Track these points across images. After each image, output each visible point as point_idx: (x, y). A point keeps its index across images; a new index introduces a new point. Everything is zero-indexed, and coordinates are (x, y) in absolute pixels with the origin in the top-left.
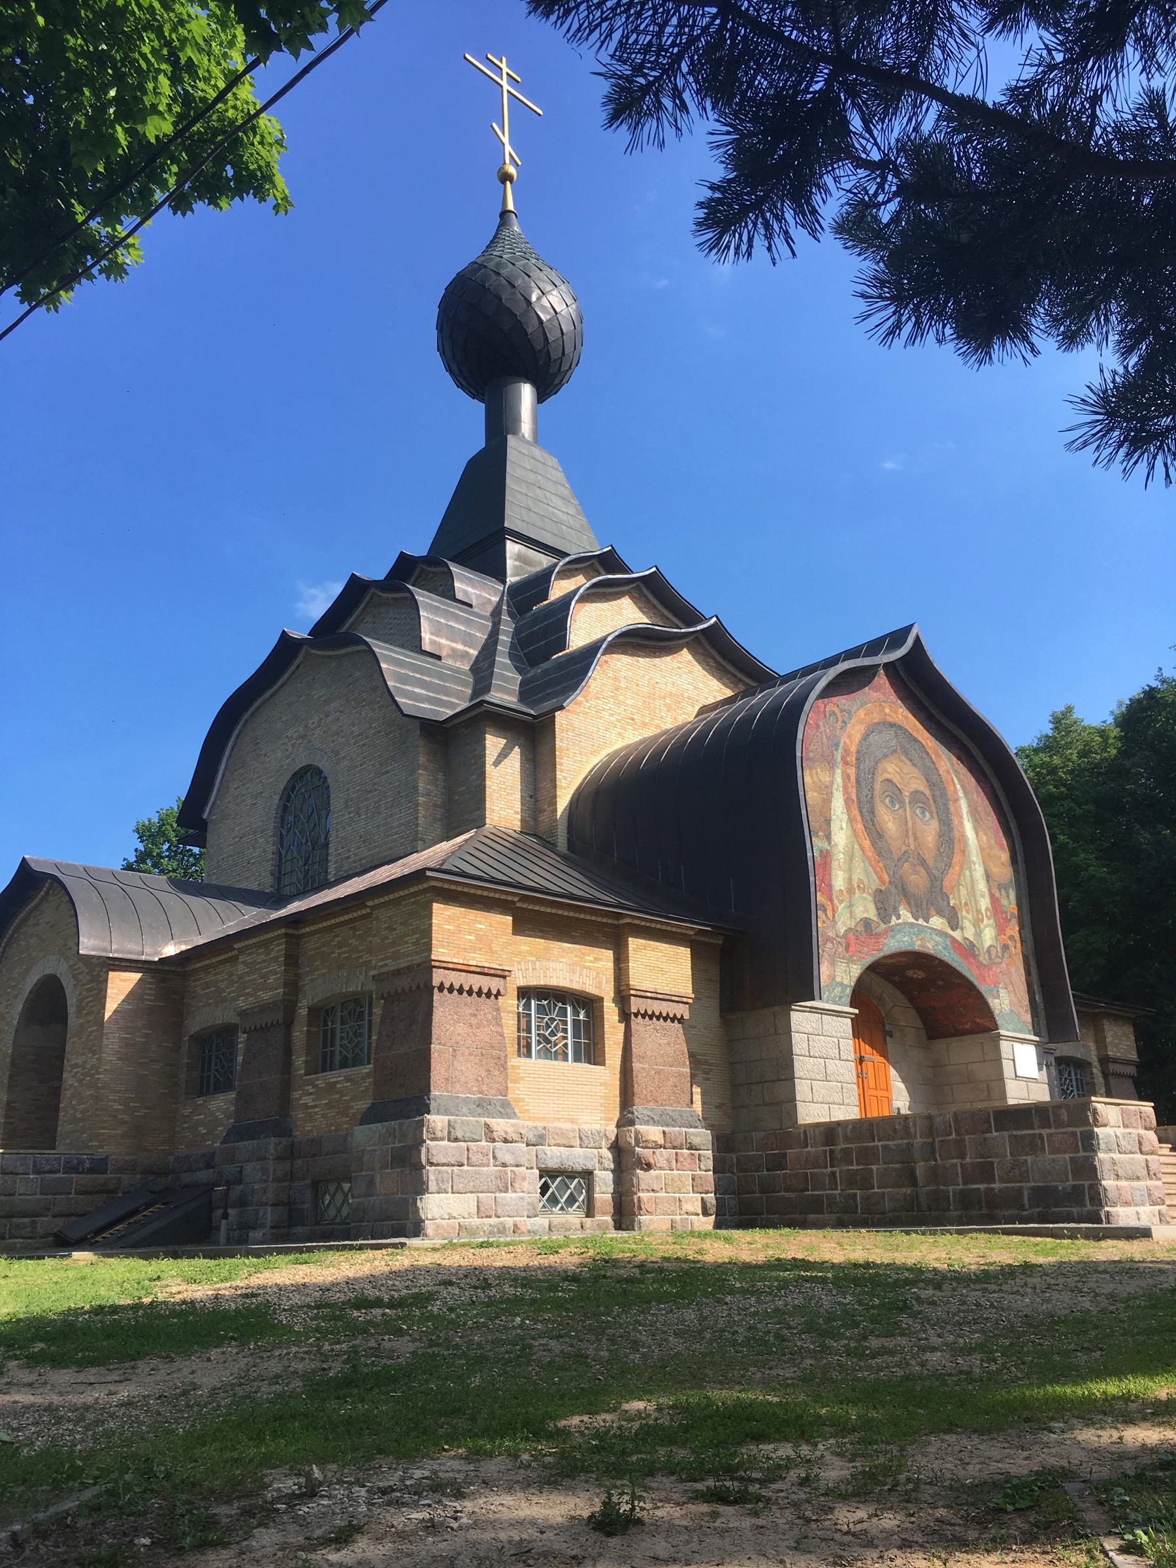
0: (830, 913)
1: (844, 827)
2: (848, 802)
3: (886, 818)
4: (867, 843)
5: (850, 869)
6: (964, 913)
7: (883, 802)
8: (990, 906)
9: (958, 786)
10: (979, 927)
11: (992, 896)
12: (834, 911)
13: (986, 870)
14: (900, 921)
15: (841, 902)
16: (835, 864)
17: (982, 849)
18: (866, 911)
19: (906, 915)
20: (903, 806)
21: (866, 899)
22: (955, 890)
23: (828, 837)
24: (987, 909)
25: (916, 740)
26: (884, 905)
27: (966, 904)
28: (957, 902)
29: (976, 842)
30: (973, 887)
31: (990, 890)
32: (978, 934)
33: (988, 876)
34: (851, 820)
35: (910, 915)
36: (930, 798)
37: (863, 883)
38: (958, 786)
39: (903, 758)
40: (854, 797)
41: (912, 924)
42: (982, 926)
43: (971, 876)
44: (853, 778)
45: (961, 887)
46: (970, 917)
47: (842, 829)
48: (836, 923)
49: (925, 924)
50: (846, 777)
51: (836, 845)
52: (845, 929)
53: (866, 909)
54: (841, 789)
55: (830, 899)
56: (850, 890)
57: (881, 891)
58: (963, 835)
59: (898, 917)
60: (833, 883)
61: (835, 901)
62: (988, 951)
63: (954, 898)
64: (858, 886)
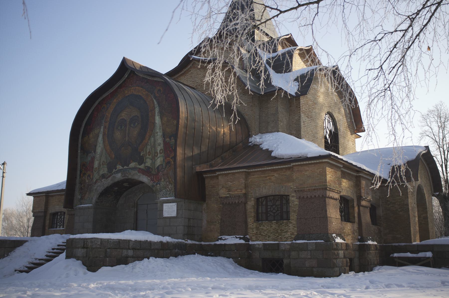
0: (91, 176)
1: (101, 145)
5: (100, 159)
6: (148, 156)
8: (163, 148)
9: (156, 103)
11: (165, 143)
13: (163, 132)
14: (117, 170)
16: (96, 159)
17: (163, 124)
19: (119, 167)
23: (95, 152)
26: (111, 167)
27: (149, 152)
28: (145, 152)
29: (160, 123)
32: (153, 163)
33: (164, 136)
34: (104, 142)
35: (121, 166)
37: (104, 162)
38: (156, 103)
40: (106, 133)
41: (122, 169)
42: (156, 158)
44: (107, 127)
46: (151, 156)
47: (100, 146)
49: (127, 167)
50: (105, 127)
53: (104, 170)
54: (102, 133)
56: (99, 165)
58: (154, 123)
59: (116, 169)
60: (94, 166)
61: (94, 172)
64: (102, 163)
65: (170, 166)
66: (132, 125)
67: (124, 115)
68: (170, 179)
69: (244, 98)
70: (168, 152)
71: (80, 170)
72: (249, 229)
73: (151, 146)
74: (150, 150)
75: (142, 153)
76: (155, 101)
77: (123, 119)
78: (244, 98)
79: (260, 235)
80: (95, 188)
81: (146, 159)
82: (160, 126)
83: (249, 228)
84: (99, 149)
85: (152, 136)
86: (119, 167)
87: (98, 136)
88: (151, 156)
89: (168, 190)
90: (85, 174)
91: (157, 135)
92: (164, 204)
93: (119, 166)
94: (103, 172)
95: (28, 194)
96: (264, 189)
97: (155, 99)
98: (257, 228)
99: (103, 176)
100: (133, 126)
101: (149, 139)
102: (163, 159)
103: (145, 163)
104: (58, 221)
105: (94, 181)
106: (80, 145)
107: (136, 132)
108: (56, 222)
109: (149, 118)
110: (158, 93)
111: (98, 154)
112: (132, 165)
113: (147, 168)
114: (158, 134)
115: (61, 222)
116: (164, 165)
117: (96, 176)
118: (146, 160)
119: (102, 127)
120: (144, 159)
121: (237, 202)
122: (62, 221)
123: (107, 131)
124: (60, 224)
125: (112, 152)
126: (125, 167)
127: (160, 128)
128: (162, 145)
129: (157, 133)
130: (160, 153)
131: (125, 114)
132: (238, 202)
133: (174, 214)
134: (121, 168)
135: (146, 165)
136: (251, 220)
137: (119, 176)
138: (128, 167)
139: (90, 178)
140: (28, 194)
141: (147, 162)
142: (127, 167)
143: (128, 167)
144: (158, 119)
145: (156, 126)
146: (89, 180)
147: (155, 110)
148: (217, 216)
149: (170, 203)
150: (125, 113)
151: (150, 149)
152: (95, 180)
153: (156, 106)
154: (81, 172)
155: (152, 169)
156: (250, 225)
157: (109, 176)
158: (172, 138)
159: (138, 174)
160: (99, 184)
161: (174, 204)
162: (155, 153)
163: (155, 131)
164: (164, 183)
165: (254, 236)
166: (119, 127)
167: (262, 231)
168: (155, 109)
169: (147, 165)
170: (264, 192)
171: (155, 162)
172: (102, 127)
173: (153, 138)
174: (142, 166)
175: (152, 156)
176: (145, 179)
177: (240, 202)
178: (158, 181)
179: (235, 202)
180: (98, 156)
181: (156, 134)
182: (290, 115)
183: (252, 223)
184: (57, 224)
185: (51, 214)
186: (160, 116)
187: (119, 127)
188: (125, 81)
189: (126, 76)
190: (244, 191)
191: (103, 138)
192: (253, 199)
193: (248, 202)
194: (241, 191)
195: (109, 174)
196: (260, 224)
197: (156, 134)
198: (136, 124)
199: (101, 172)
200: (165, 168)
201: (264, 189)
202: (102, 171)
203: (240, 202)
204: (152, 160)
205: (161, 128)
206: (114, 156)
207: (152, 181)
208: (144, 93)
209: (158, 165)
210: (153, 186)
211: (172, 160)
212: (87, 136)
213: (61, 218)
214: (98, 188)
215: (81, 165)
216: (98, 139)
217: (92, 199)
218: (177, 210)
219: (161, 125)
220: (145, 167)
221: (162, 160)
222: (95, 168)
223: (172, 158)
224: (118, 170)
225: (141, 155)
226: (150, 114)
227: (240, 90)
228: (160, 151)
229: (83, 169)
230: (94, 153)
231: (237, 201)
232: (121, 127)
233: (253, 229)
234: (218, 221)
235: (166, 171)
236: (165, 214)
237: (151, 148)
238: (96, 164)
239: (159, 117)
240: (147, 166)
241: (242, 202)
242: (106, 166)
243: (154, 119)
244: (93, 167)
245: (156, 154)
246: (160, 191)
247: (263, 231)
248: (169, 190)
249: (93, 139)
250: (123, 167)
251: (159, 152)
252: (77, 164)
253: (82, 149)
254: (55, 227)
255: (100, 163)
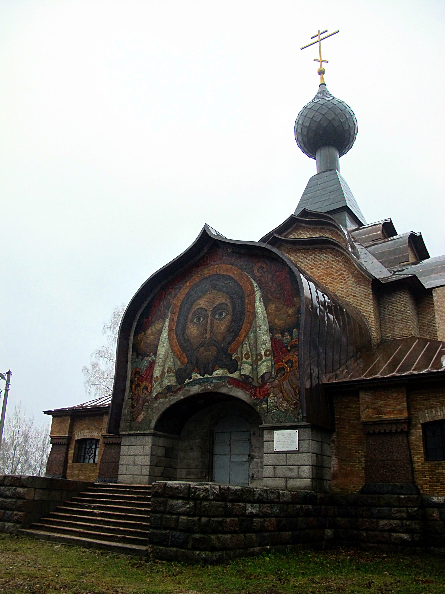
0: (149, 389)
1: (165, 344)
2: (170, 331)
3: (192, 329)
4: (177, 348)
5: (164, 364)
6: (244, 360)
7: (192, 321)
9: (255, 285)
10: (257, 364)
12: (151, 388)
13: (270, 326)
14: (192, 380)
15: (155, 382)
16: (157, 365)
17: (269, 314)
18: (170, 381)
20: (206, 317)
21: (171, 376)
22: (239, 350)
23: (155, 354)
24: (266, 351)
25: (224, 276)
27: (247, 354)
30: (256, 342)
31: (271, 338)
32: (255, 370)
33: (272, 330)
36: (229, 304)
37: (171, 369)
39: (213, 291)
40: (174, 328)
41: (201, 379)
42: (259, 363)
43: (255, 336)
44: (176, 319)
45: (244, 346)
47: (164, 346)
48: (152, 393)
49: (209, 376)
50: (172, 320)
51: (159, 356)
52: (156, 394)
54: (167, 328)
55: (151, 382)
57: (181, 369)
58: (254, 314)
60: (154, 374)
62: (263, 376)
63: (238, 355)
65: (284, 374)
66: (217, 316)
67: (202, 303)
68: (285, 394)
69: (359, 289)
70: (281, 353)
71: (131, 380)
72: (418, 473)
73: (250, 345)
74: (248, 351)
75: (235, 355)
76: (254, 282)
77: (200, 308)
78: (359, 289)
79: (437, 482)
80: (155, 405)
81: (241, 364)
82: (264, 317)
83: (416, 471)
84: (161, 351)
85: (250, 332)
86: (196, 376)
87: (160, 332)
88: (249, 360)
89: (281, 411)
90: (138, 385)
91: (260, 330)
92: (275, 431)
93: (196, 374)
94: (168, 383)
95: (46, 413)
96: (439, 410)
97: (254, 279)
98: (431, 472)
99: (169, 389)
100: (218, 318)
101: (246, 336)
102: (272, 364)
103: (240, 370)
104: (86, 452)
105: (154, 395)
106: (131, 345)
107: (224, 325)
108: (83, 454)
109: (246, 306)
110: (258, 272)
111: (161, 357)
112: (218, 373)
113: (243, 377)
114: (261, 328)
115: (92, 454)
116: (273, 373)
117: (156, 389)
118: (241, 365)
119: (168, 320)
120: (238, 364)
121: (393, 430)
122: (93, 452)
123: (175, 325)
124: (90, 456)
125: (184, 355)
126: (206, 376)
127: (264, 320)
128: (269, 345)
129: (260, 326)
130: (266, 355)
131: (205, 301)
132: (396, 430)
133: (295, 447)
134: (199, 377)
135: (242, 373)
136: (418, 459)
137: (195, 389)
138: (210, 376)
139: (148, 391)
140: (46, 413)
141: (243, 368)
142: (209, 376)
143: (210, 376)
144: (259, 307)
145: (258, 317)
146: (145, 394)
147: (255, 295)
148: (356, 452)
149: (286, 429)
150: (204, 299)
151: (249, 351)
152: (154, 395)
153: (256, 289)
154: (132, 382)
155: (252, 379)
156: (418, 466)
157: (180, 389)
158: (286, 333)
159: (229, 386)
160: (162, 400)
161: (294, 431)
162: (257, 355)
163: (256, 324)
164: (275, 400)
165: (426, 484)
166: (195, 320)
167: (441, 476)
168: (254, 292)
169: (242, 372)
170: (440, 415)
171: (257, 369)
172: (168, 320)
173: (252, 334)
174: (235, 375)
175: (252, 360)
176: (240, 394)
177: (399, 430)
178: (264, 397)
179: (391, 430)
180: (160, 360)
181: (258, 329)
182: (418, 314)
183: (422, 464)
184: (84, 456)
185: (76, 441)
186: (264, 303)
187: (195, 320)
188: (203, 257)
189: (206, 251)
190: (406, 414)
191: (169, 335)
192: (420, 426)
193: (411, 431)
194: (401, 414)
195: (179, 386)
196: (437, 465)
197: (257, 328)
198: (224, 314)
199: (166, 383)
200: (276, 376)
201: (439, 410)
202: (167, 381)
203: (399, 430)
204: (252, 365)
205: (266, 319)
206: (186, 360)
207: (252, 397)
208: (235, 272)
209: (262, 373)
210: (256, 404)
211: (287, 366)
212: (143, 333)
213: (91, 447)
214: (160, 406)
215: (132, 373)
216: (160, 336)
217: (150, 421)
218: (299, 440)
219: (266, 315)
220: (241, 375)
221: (270, 365)
222: (155, 376)
223: (286, 363)
224: (194, 380)
225: (233, 358)
226: (246, 301)
227: (352, 278)
228: (265, 352)
229: (136, 379)
230: (153, 356)
231: (395, 429)
232: (199, 320)
233: (423, 472)
234: (359, 460)
235: (276, 382)
236: (278, 447)
237: (250, 348)
238: (157, 372)
239: (263, 303)
240: (243, 375)
241: (402, 430)
242: (173, 375)
243: (254, 307)
244: (152, 376)
245: (259, 357)
246: (268, 412)
247: (443, 476)
248: (284, 409)
249: (152, 337)
250: (204, 376)
251: (263, 354)
252: (127, 371)
253: (135, 349)
254: (82, 461)
255: (164, 369)
